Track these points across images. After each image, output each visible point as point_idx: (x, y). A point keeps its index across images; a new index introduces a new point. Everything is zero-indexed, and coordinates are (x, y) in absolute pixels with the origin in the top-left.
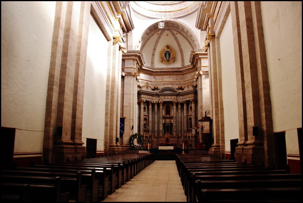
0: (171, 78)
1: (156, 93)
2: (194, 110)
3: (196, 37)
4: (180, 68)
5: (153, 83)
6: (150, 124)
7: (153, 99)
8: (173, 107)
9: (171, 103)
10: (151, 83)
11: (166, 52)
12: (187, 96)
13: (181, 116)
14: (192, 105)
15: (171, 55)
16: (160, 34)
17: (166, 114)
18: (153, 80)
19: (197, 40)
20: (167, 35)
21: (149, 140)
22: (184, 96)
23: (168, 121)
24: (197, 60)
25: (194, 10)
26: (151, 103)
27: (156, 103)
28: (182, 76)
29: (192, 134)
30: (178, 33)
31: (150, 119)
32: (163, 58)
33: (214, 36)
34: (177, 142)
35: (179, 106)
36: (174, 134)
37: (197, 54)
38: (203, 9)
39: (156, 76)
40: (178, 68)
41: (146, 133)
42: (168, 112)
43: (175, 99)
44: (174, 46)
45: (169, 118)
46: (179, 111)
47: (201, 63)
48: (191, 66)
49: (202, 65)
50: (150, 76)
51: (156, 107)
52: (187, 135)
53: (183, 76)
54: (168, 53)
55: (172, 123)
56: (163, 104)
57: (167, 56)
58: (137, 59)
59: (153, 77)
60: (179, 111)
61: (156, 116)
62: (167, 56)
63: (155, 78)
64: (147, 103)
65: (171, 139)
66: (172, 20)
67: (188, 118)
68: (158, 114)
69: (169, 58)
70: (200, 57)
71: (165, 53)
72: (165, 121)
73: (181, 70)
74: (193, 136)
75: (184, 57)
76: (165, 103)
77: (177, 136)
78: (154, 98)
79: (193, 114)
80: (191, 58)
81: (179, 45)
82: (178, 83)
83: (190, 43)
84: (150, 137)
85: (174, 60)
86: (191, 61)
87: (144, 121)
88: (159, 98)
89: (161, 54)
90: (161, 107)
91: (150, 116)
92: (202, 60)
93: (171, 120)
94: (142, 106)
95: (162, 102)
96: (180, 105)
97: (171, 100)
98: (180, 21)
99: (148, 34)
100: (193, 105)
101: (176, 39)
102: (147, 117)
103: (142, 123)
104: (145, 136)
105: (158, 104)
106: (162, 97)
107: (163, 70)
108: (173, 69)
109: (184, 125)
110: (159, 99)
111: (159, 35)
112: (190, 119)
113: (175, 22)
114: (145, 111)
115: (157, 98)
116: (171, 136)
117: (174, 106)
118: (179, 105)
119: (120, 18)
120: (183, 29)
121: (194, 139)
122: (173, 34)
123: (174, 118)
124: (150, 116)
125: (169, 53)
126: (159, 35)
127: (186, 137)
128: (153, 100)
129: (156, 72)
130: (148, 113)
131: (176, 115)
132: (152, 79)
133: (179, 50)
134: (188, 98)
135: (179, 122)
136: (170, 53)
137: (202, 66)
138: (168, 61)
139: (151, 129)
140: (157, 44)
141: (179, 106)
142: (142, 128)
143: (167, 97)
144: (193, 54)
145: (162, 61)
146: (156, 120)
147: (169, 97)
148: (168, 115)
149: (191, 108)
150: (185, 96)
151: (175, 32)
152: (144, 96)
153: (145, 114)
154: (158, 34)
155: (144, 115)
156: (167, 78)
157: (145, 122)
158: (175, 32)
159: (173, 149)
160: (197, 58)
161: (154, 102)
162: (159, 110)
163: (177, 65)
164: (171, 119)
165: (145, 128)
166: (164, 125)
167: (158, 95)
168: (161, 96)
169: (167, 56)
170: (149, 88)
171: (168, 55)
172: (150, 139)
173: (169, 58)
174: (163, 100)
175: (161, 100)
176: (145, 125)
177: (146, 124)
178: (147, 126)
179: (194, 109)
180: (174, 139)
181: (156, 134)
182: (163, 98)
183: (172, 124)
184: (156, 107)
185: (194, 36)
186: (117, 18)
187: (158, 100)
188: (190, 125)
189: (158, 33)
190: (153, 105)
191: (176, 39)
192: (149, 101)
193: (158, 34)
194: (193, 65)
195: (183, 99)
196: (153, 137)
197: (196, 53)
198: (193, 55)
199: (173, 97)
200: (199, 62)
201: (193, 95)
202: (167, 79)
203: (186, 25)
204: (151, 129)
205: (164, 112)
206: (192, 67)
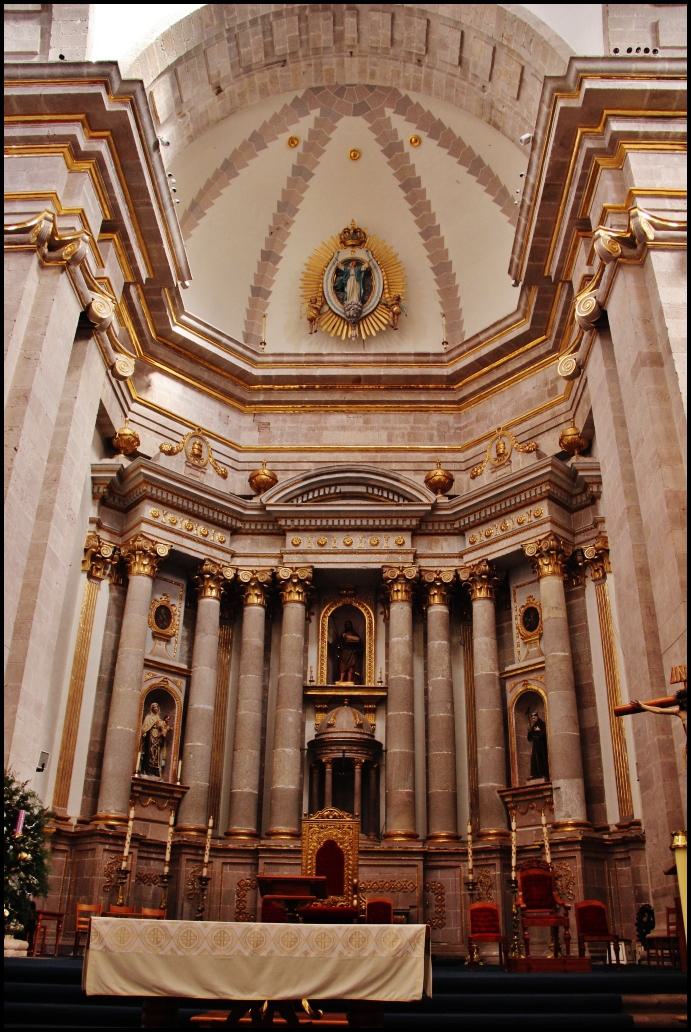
0: (372, 429)
1: (263, 507)
2: (562, 625)
4: (437, 359)
5: (242, 457)
6: (199, 743)
7: (234, 555)
8: (387, 620)
9: (373, 586)
10: (233, 453)
11: (347, 262)
12: (495, 529)
13: (451, 685)
14: (544, 582)
16: (308, 147)
17: (335, 676)
18: (249, 438)
20: (355, 155)
21: (172, 878)
22: (469, 536)
23: (344, 722)
26: (217, 581)
27: (259, 585)
28: (450, 419)
29: (556, 827)
30: (423, 135)
31: (203, 702)
34: (424, 899)
35: (437, 610)
36: (397, 825)
39: (264, 419)
40: (422, 358)
41: (151, 812)
42: (347, 655)
43: (400, 558)
44: (397, 233)
45: (354, 702)
46: (438, 643)
49: (639, 182)
50: (226, 411)
51: (255, 611)
52: (505, 836)
53: (458, 418)
55: (380, 744)
56: (305, 588)
57: (348, 289)
58: (102, 147)
59: (248, 420)
60: (438, 643)
61: (251, 681)
62: (352, 286)
63: (263, 427)
64: (181, 570)
65: (366, 875)
67: (511, 698)
68: (266, 674)
69: (363, 300)
70: (616, 126)
71: (338, 272)
72: (318, 728)
73: (447, 371)
74: (563, 843)
75: (462, 305)
76: (322, 587)
77: (417, 846)
78: (243, 545)
79: (555, 652)
81: (429, 232)
82: (426, 457)
84: (189, 845)
85: (397, 314)
87: (147, 708)
88: (284, 544)
89: (312, 279)
90: (294, 612)
91: (205, 675)
93: (370, 719)
94: (141, 583)
95: (306, 574)
96: (445, 601)
97: (373, 562)
99: (219, 91)
100: (549, 589)
101: (410, 185)
102: (176, 686)
103: (126, 722)
104: (135, 838)
105: (274, 592)
106: (308, 541)
107: (318, 372)
108: (390, 363)
109: (473, 762)
110: (280, 557)
111: (300, 148)
112: (531, 701)
114: (167, 639)
115: (269, 545)
116: (365, 843)
117: (395, 609)
118: (437, 599)
120: (460, 63)
121: (579, 866)
122: (393, 150)
123: (396, 696)
124: (205, 675)
125: (363, 268)
126: (300, 148)
127: (504, 852)
128: (238, 561)
129: (267, 379)
130: (190, 664)
131: (412, 674)
132: (242, 429)
133: (428, 264)
134: (504, 543)
135: (438, 734)
136: (368, 273)
138: (356, 320)
139: (197, 779)
140: (288, 224)
141: (437, 610)
142: (120, 763)
143: (338, 541)
144: (561, 104)
145: (311, 320)
146: (249, 712)
147: (359, 541)
148: (350, 684)
149: (532, 618)
150: (478, 535)
151: (404, 129)
152: (168, 517)
153: (157, 659)
155: (149, 665)
156: (344, 428)
157: (152, 719)
158: (404, 129)
159: (409, 985)
160: (589, 144)
161: (244, 577)
162: (280, 633)
163: (426, 336)
164: (373, 711)
165: (147, 766)
166: (314, 754)
167: (273, 526)
168: (296, 530)
169: (352, 286)
170: (210, 470)
172: (187, 869)
173: (363, 300)
174: (310, 557)
175: (295, 558)
176: (148, 747)
177: (165, 741)
178: (174, 756)
179: (561, 614)
180: (396, 872)
181: (244, 826)
182: (315, 547)
183: (374, 750)
184: (255, 611)
187: (274, 562)
188: (528, 752)
190: (233, 597)
191: (410, 185)
192: (202, 562)
193: (293, 142)
195: (460, 556)
196: (211, 850)
198: (562, 109)
199: (389, 541)
201: (544, 509)
202: (347, 434)
204: (197, 779)
205: (320, 658)
206: (526, 327)
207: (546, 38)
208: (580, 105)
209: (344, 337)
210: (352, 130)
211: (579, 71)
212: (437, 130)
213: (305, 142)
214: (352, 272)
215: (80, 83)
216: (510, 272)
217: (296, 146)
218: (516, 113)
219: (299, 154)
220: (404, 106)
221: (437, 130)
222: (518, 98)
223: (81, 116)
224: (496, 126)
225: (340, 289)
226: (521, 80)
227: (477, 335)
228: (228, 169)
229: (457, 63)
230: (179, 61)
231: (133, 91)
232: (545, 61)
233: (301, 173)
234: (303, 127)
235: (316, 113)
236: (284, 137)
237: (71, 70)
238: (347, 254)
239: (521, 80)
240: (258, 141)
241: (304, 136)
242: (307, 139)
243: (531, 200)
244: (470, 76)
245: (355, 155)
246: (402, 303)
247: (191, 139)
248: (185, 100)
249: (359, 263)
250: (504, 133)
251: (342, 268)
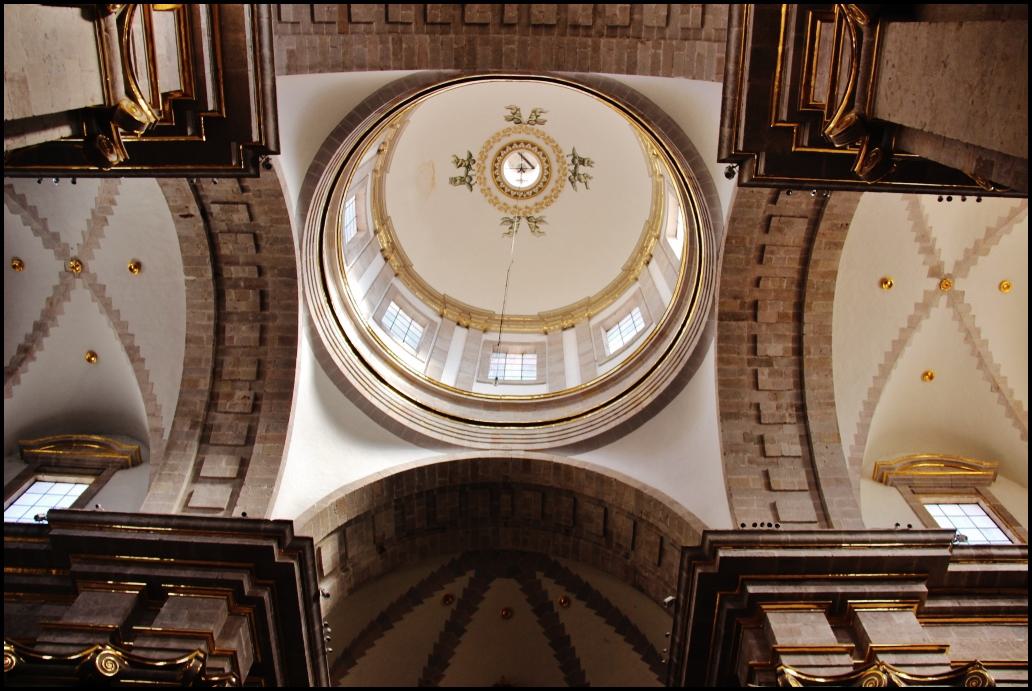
20: (508, 614)
30: (572, 597)
49: (781, 640)
98: (587, 464)
111: (454, 606)
122: (543, 609)
144: (699, 571)
151: (555, 592)
158: (555, 592)
160: (729, 606)
189: (449, 588)
193: (448, 599)
198: (700, 574)
203: (629, 478)
207: (680, 514)
208: (716, 570)
210: (503, 591)
211: (712, 542)
212: (585, 593)
213: (459, 600)
215: (256, 537)
217: (451, 603)
218: (658, 577)
219: (453, 611)
220: (554, 571)
221: (585, 593)
222: (660, 564)
223: (251, 565)
224: (642, 590)
226: (662, 550)
228: (383, 622)
229: (601, 533)
230: (348, 524)
231: (303, 548)
232: (681, 533)
233: (453, 631)
234: (458, 586)
235: (471, 574)
236: (440, 595)
237: (250, 525)
239: (662, 550)
240: (414, 597)
241: (459, 594)
242: (461, 597)
243: (678, 659)
244: (614, 545)
245: (508, 614)
247: (351, 591)
248: (350, 556)
250: (649, 596)
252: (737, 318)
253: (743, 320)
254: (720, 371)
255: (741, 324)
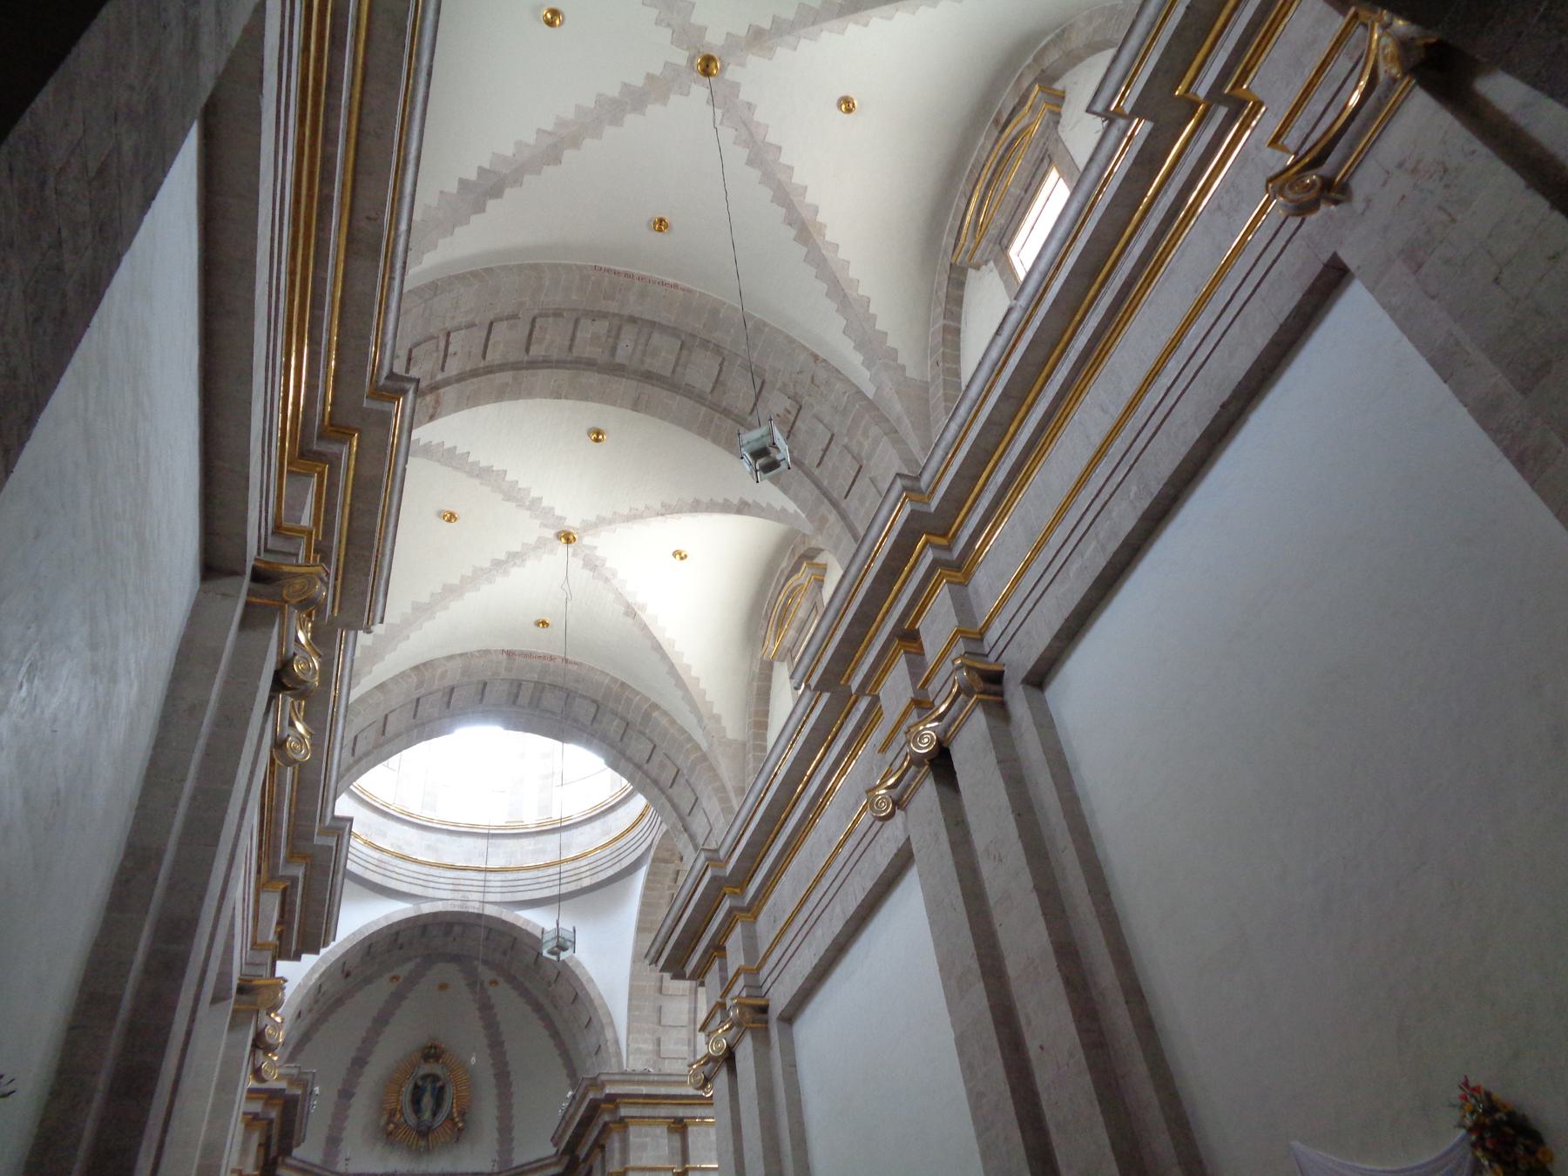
3: (605, 1005)
11: (424, 1078)
15: (450, 1092)
19: (612, 1023)
24: (605, 1129)
25: (610, 872)
30: (501, 980)
32: (402, 1114)
33: (764, 1010)
37: (611, 1098)
38: (714, 879)
47: (625, 1150)
48: (556, 1164)
49: (632, 1163)
54: (434, 1089)
66: (490, 911)
69: (434, 1114)
71: (416, 1087)
80: (572, 1117)
81: (496, 1044)
83: (555, 1034)
86: (561, 1137)
92: (632, 1130)
98: (528, 922)
99: (347, 975)
101: (486, 1008)
113: (504, 922)
119: (294, 880)
122: (473, 982)
125: (439, 1084)
136: (442, 1088)
137: (632, 1163)
151: (486, 974)
154: (395, 978)
160: (606, 1118)
169: (427, 1101)
171: (432, 1095)
173: (434, 1114)
185: (596, 1003)
186: (283, 878)
189: (396, 972)
191: (486, 1008)
194: (566, 1160)
197: (609, 1090)
200: (616, 1144)
209: (414, 1147)
214: (429, 1088)
216: (551, 1140)
225: (416, 1101)
227: (522, 1166)
233: (398, 997)
236: (388, 976)
238: (426, 1069)
246: (467, 1116)
249: (435, 1078)
251: (420, 1083)
252: (665, 861)
253: (670, 863)
254: (644, 896)
255: (669, 865)
